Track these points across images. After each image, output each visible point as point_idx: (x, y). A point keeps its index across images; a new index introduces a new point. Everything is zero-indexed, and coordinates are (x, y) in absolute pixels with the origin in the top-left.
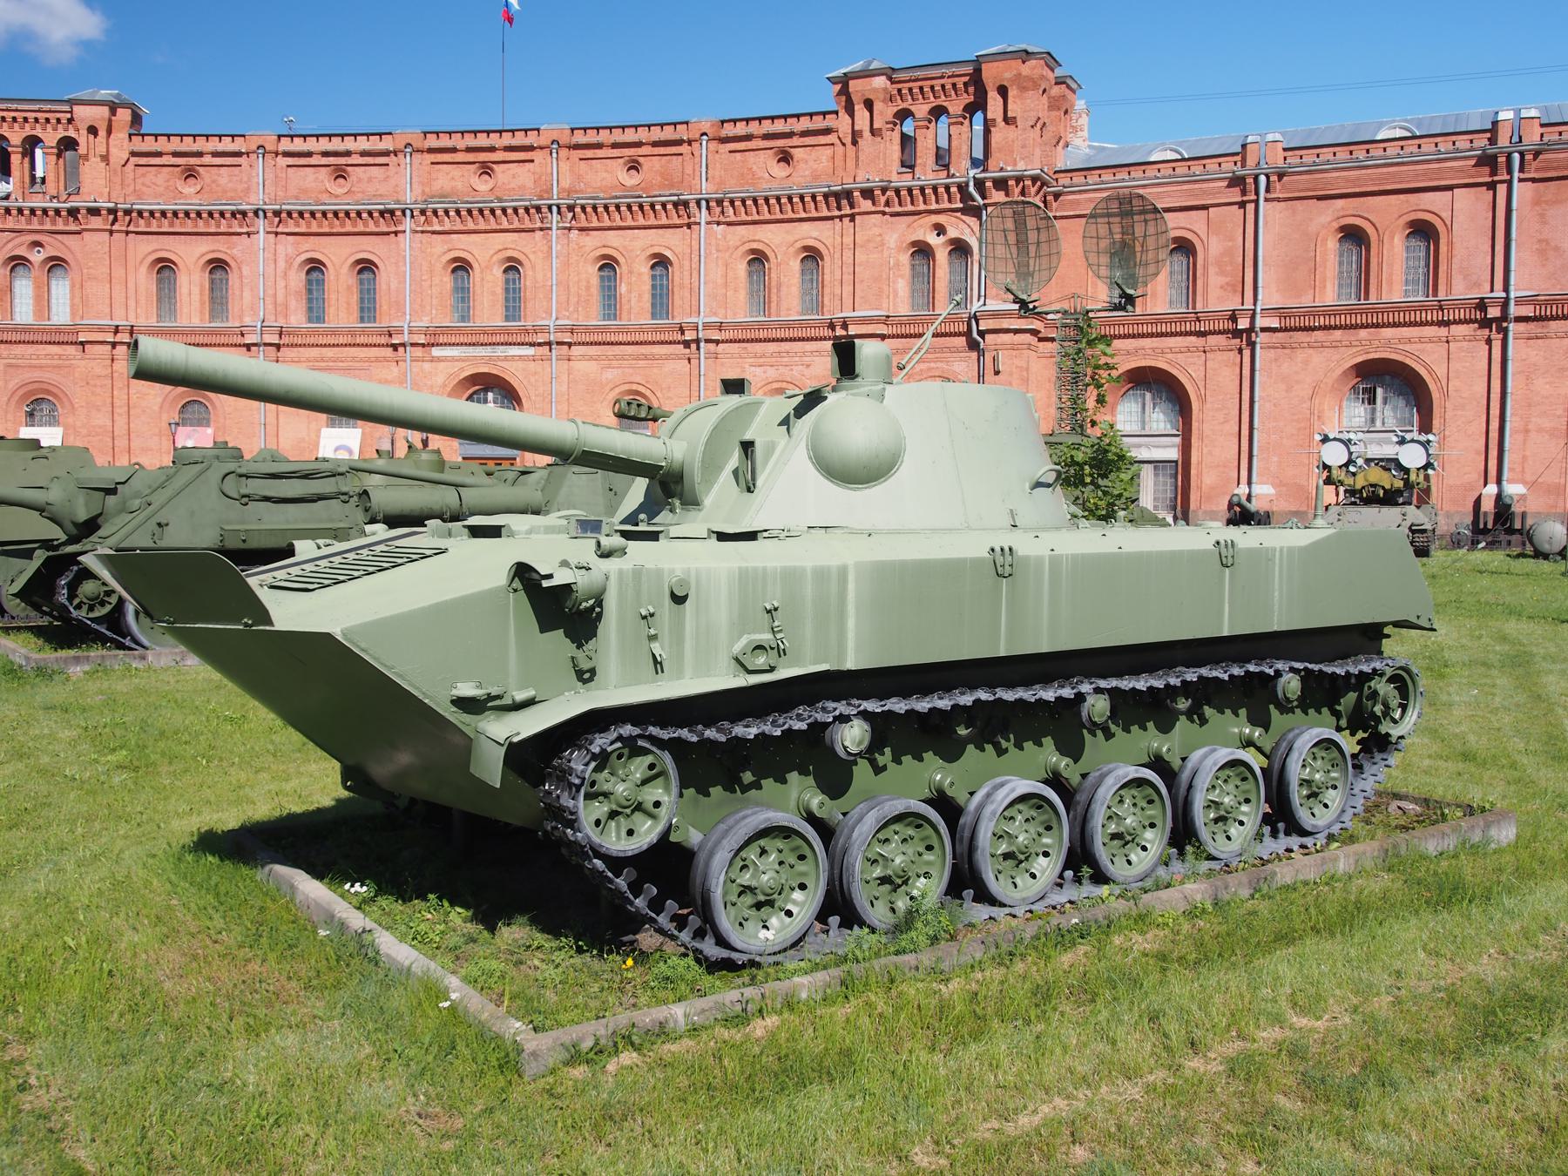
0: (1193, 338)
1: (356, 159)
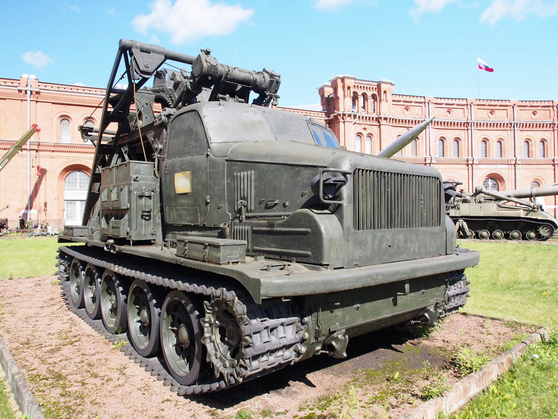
1: (455, 106)
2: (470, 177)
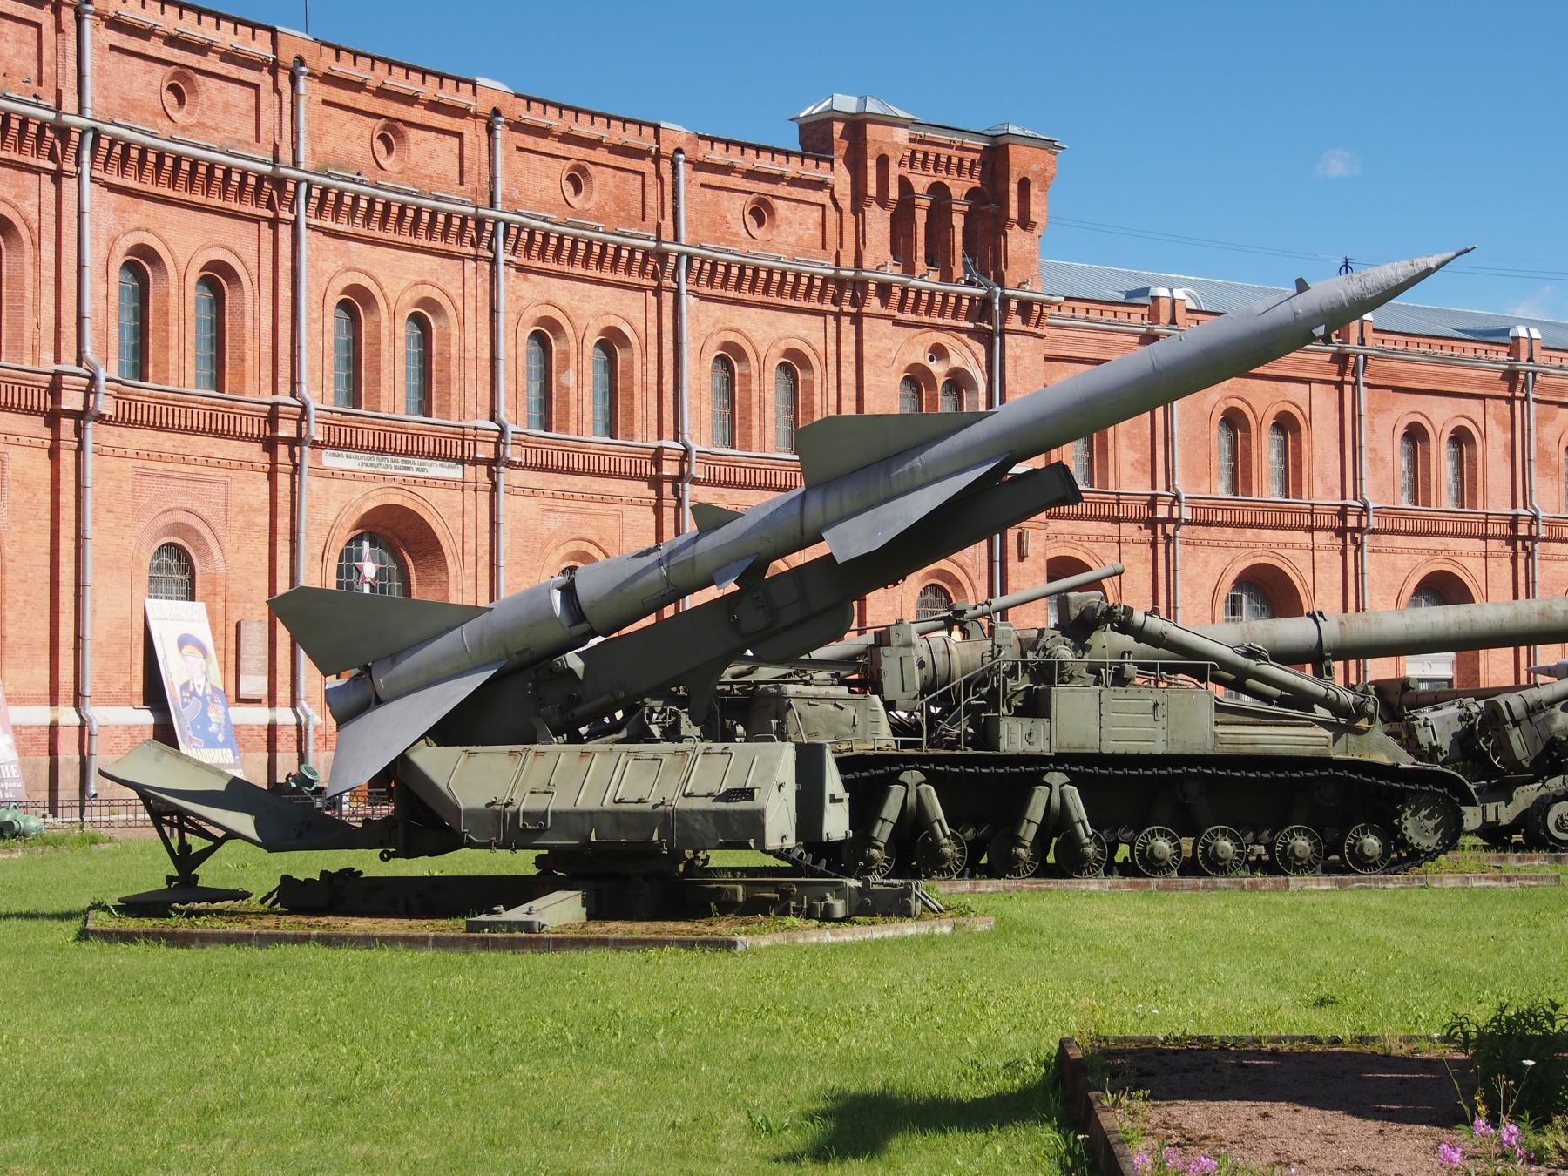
0: (1106, 525)
1: (212, 63)
2: (283, 522)
